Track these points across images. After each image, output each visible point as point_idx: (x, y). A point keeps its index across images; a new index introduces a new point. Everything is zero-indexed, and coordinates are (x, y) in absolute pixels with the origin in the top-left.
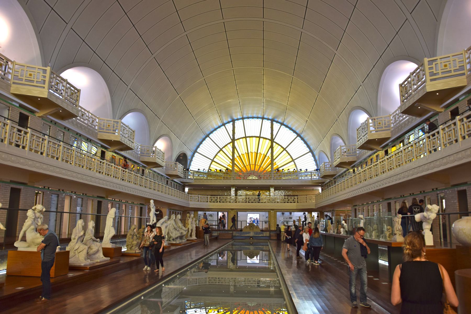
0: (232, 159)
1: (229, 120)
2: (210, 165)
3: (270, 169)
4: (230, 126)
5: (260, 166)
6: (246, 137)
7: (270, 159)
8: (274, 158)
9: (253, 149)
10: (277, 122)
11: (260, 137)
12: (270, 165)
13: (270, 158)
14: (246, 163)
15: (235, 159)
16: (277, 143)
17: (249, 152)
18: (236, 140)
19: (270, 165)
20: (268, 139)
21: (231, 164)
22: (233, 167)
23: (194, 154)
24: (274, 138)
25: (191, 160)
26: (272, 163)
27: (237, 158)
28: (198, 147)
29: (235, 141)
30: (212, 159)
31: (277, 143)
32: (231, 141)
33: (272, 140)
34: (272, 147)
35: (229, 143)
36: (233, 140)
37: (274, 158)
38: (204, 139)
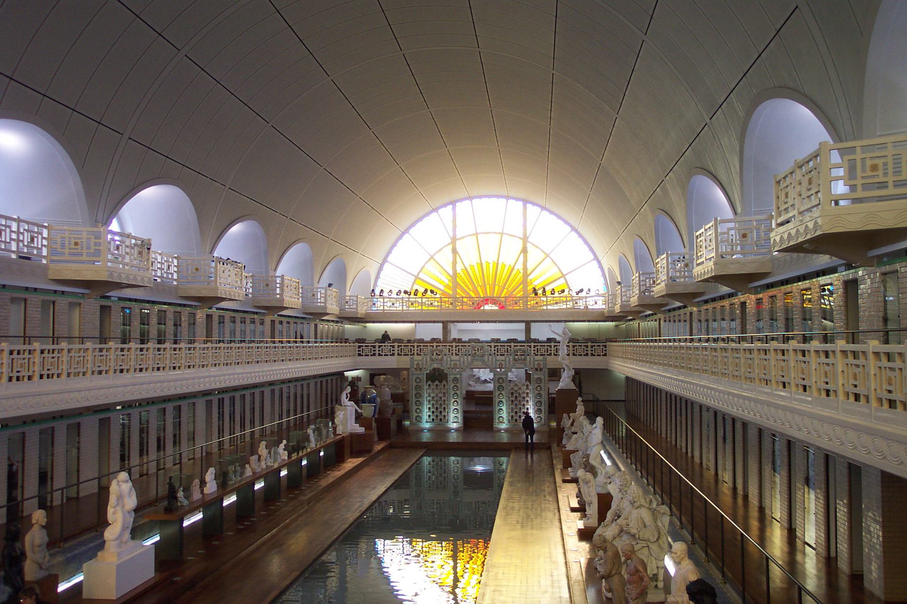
0: (451, 273)
1: (447, 200)
2: (413, 286)
3: (522, 293)
4: (447, 212)
5: (504, 288)
6: (476, 234)
7: (521, 275)
8: (528, 273)
9: (489, 257)
10: (533, 204)
11: (502, 234)
12: (522, 286)
13: (522, 271)
14: (478, 281)
15: (458, 275)
16: (533, 245)
17: (483, 262)
18: (459, 239)
19: (522, 286)
20: (518, 237)
21: (451, 284)
22: (454, 290)
23: (382, 265)
24: (528, 235)
25: (377, 277)
26: (525, 281)
27: (461, 274)
28: (389, 252)
29: (457, 242)
30: (416, 274)
31: (533, 245)
32: (450, 241)
33: (525, 239)
34: (524, 251)
35: (447, 245)
36: (454, 240)
37: (529, 272)
38: (400, 237)
